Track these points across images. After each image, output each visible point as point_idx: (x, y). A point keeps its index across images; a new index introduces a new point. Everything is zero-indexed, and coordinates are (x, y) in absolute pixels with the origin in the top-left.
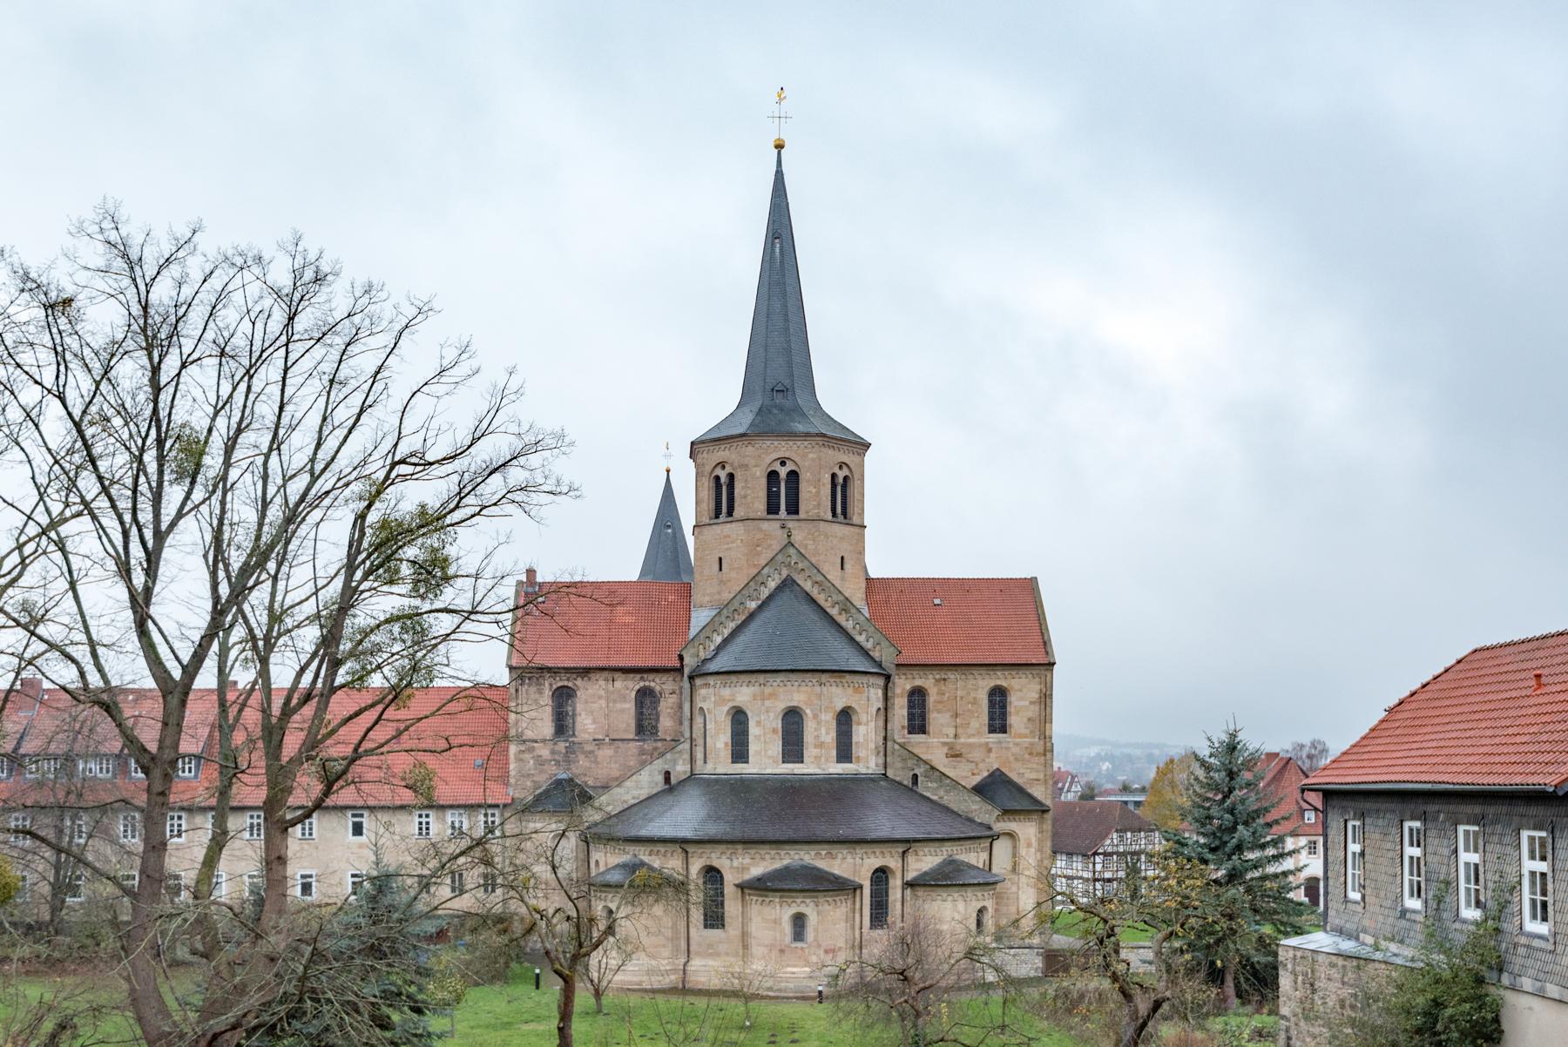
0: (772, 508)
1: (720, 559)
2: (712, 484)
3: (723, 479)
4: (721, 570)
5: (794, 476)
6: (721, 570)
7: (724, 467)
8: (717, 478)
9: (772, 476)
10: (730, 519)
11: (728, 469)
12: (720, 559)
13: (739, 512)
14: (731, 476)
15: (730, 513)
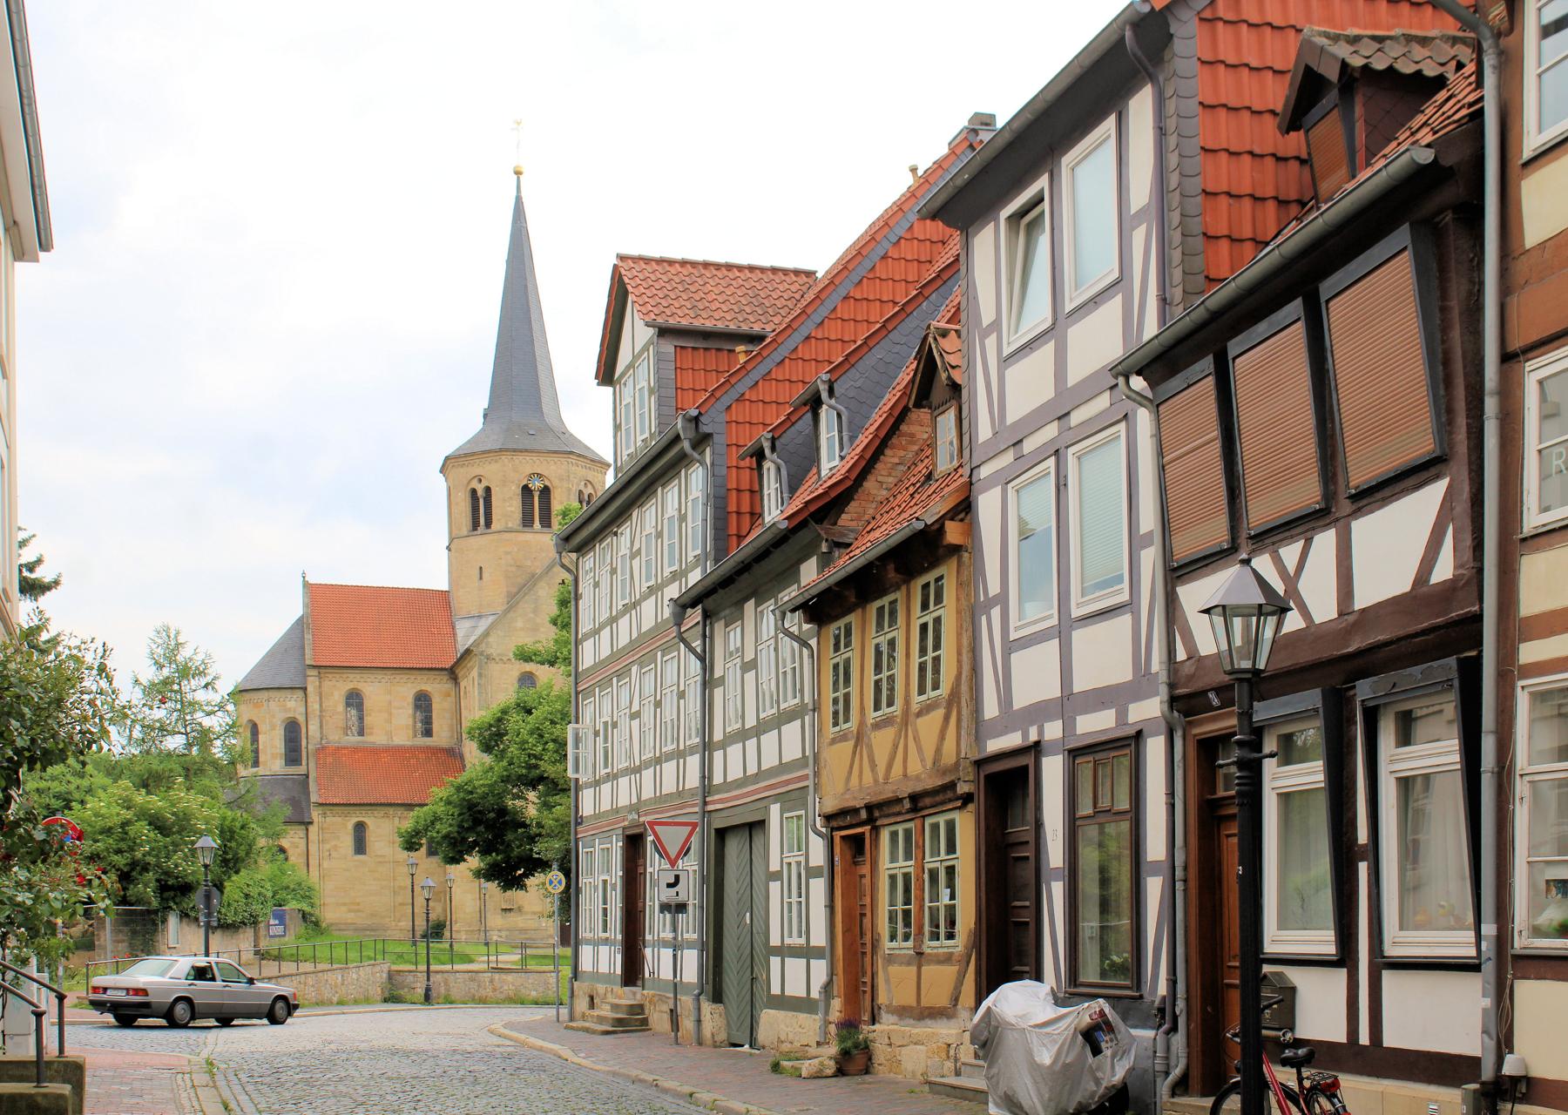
0: (527, 521)
1: (481, 568)
2: (468, 496)
3: (480, 493)
4: (481, 578)
5: (546, 492)
6: (481, 578)
7: (480, 481)
8: (474, 492)
9: (526, 490)
10: (489, 531)
11: (485, 483)
12: (481, 568)
13: (495, 526)
14: (488, 490)
15: (488, 524)
